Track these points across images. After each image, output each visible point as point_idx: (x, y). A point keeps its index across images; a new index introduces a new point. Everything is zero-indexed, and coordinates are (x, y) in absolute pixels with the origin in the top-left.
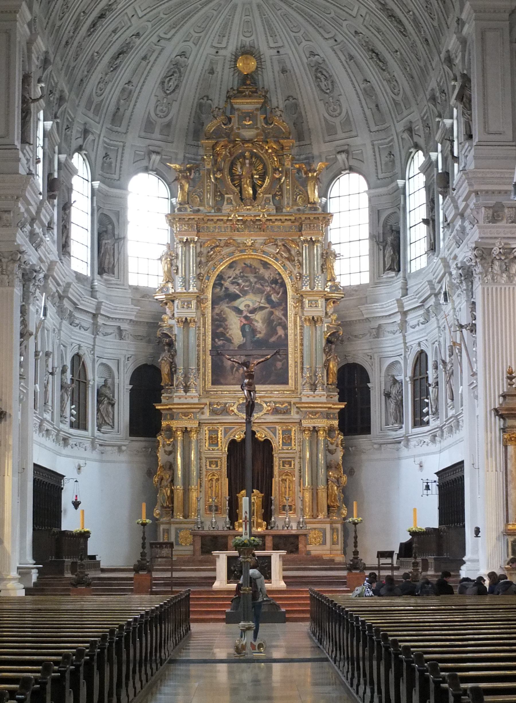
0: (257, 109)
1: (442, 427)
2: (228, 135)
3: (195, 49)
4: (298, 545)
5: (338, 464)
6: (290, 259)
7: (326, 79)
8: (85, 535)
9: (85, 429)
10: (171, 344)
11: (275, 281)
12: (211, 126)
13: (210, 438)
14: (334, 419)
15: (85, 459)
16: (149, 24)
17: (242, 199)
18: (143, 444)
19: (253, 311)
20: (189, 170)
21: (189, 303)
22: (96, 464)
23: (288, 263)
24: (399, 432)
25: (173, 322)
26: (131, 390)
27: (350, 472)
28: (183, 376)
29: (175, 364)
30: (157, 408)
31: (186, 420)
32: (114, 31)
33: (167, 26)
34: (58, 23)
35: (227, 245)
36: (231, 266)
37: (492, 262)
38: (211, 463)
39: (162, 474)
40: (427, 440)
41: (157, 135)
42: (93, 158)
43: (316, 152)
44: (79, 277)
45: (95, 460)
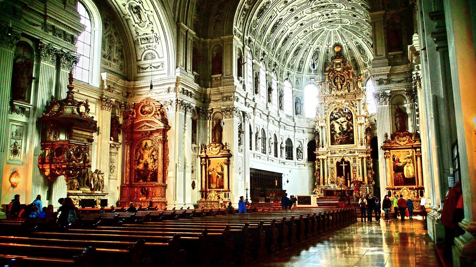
0: (341, 62)
2: (332, 71)
3: (321, 46)
6: (353, 106)
7: (362, 50)
8: (286, 191)
9: (292, 159)
10: (318, 134)
11: (349, 113)
12: (327, 69)
13: (331, 161)
14: (369, 154)
16: (305, 41)
17: (338, 89)
18: (311, 164)
19: (342, 123)
20: (322, 82)
21: (323, 121)
23: (352, 107)
25: (318, 127)
32: (293, 44)
33: (311, 41)
34: (267, 43)
35: (333, 103)
36: (335, 109)
37: (380, 98)
38: (331, 169)
41: (313, 73)
42: (292, 82)
43: (362, 73)
44: (287, 116)
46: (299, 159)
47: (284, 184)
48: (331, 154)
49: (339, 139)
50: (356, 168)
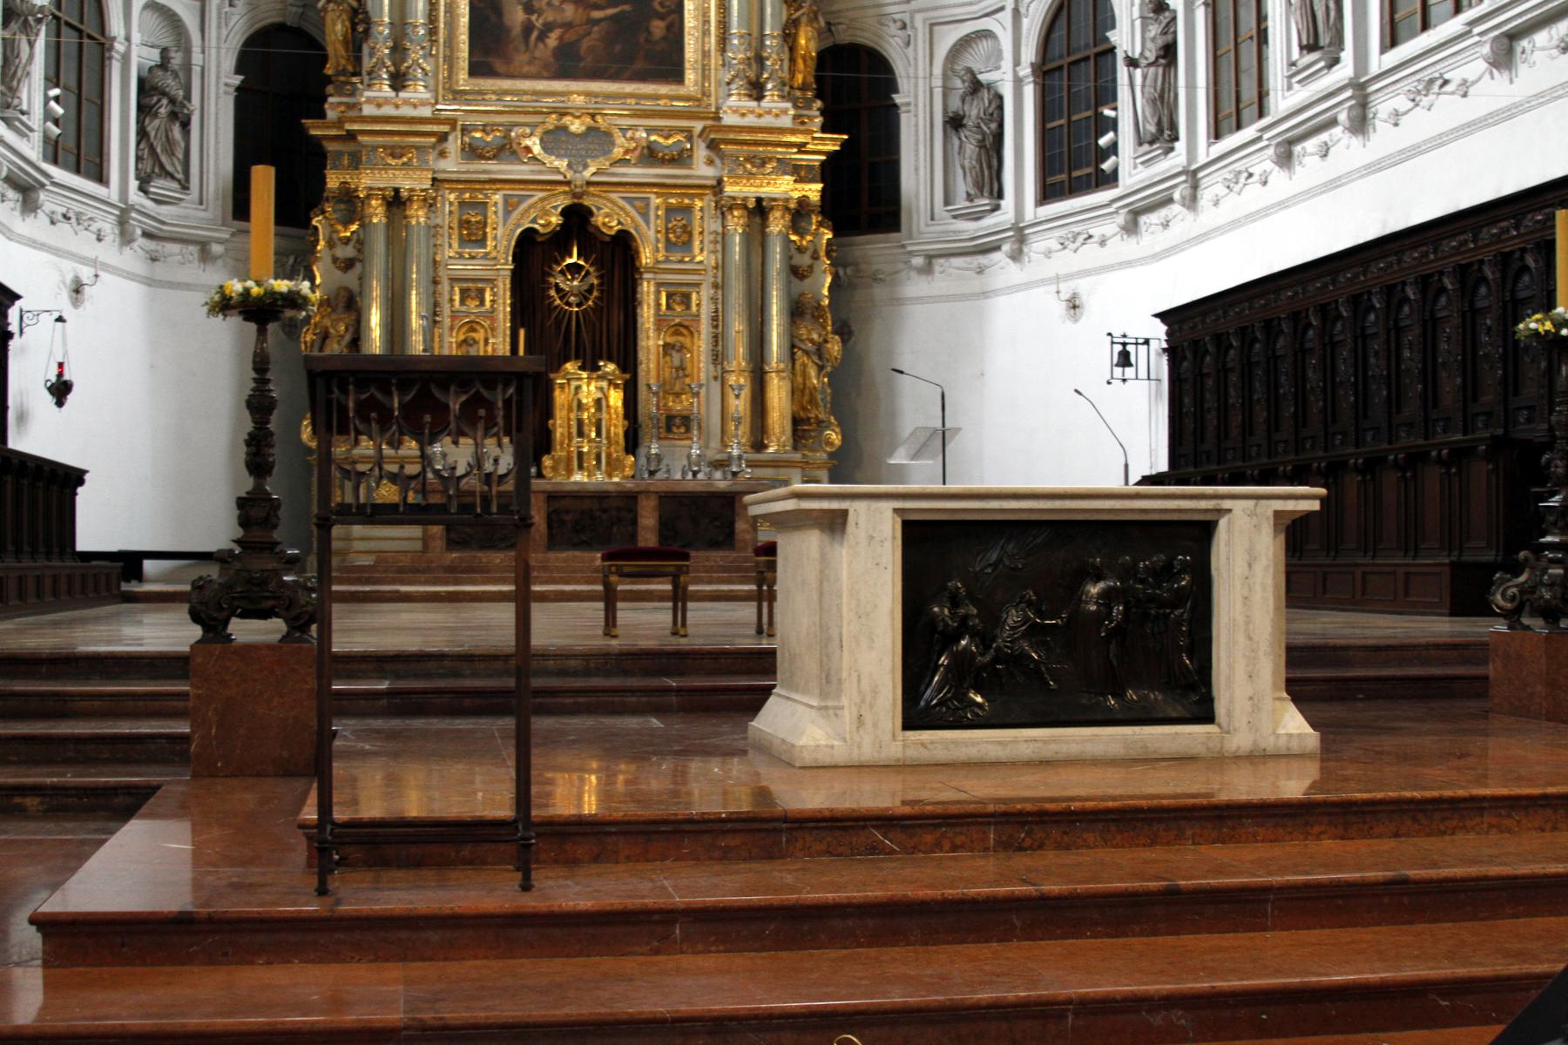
1: (1195, 172)
4: (732, 524)
5: (819, 307)
9: (101, 177)
13: (464, 224)
15: (93, 262)
22: (134, 289)
24: (990, 222)
26: (238, 89)
27: (844, 331)
28: (390, 44)
29: (366, 13)
30: (313, 132)
31: (395, 168)
38: (465, 294)
39: (327, 322)
40: (1111, 227)
45: (130, 276)
46: (159, 186)
47: (22, 418)
48: (473, 152)
49: (548, 28)
50: (686, 299)
